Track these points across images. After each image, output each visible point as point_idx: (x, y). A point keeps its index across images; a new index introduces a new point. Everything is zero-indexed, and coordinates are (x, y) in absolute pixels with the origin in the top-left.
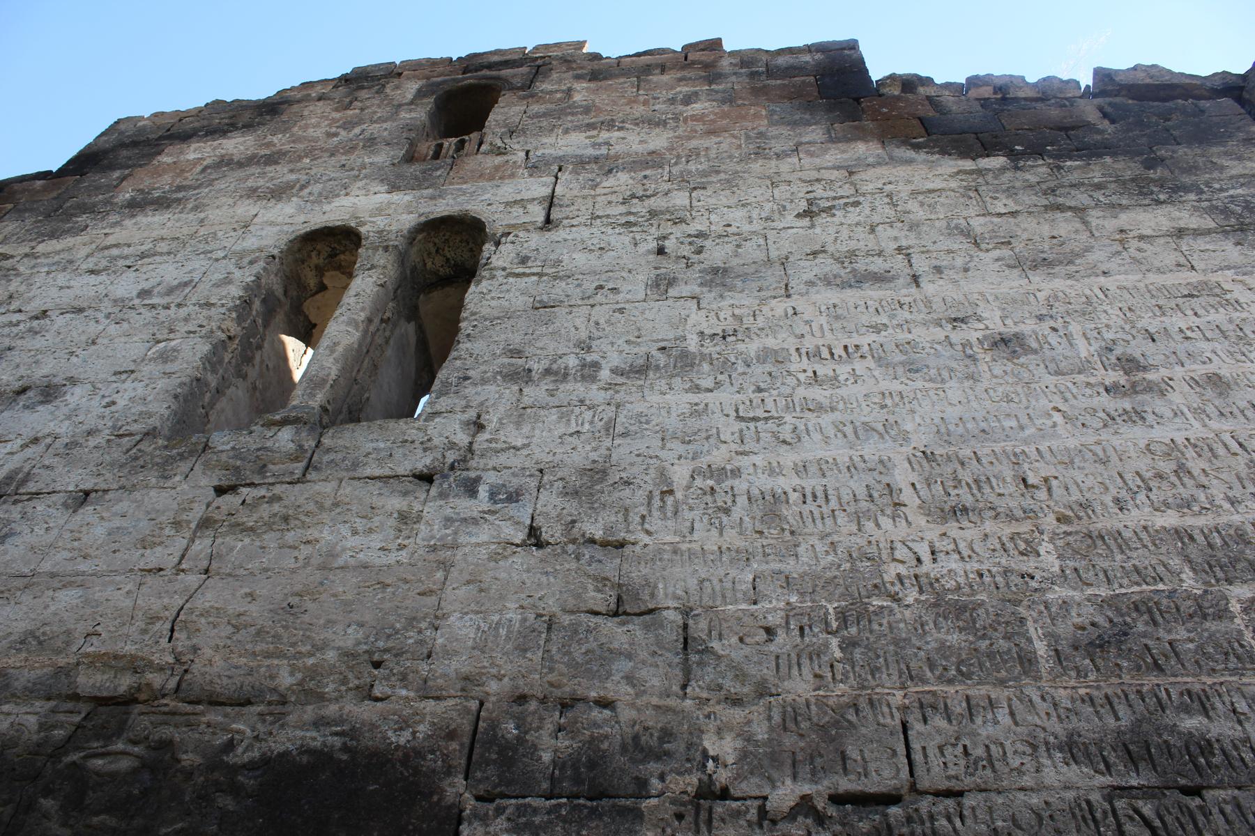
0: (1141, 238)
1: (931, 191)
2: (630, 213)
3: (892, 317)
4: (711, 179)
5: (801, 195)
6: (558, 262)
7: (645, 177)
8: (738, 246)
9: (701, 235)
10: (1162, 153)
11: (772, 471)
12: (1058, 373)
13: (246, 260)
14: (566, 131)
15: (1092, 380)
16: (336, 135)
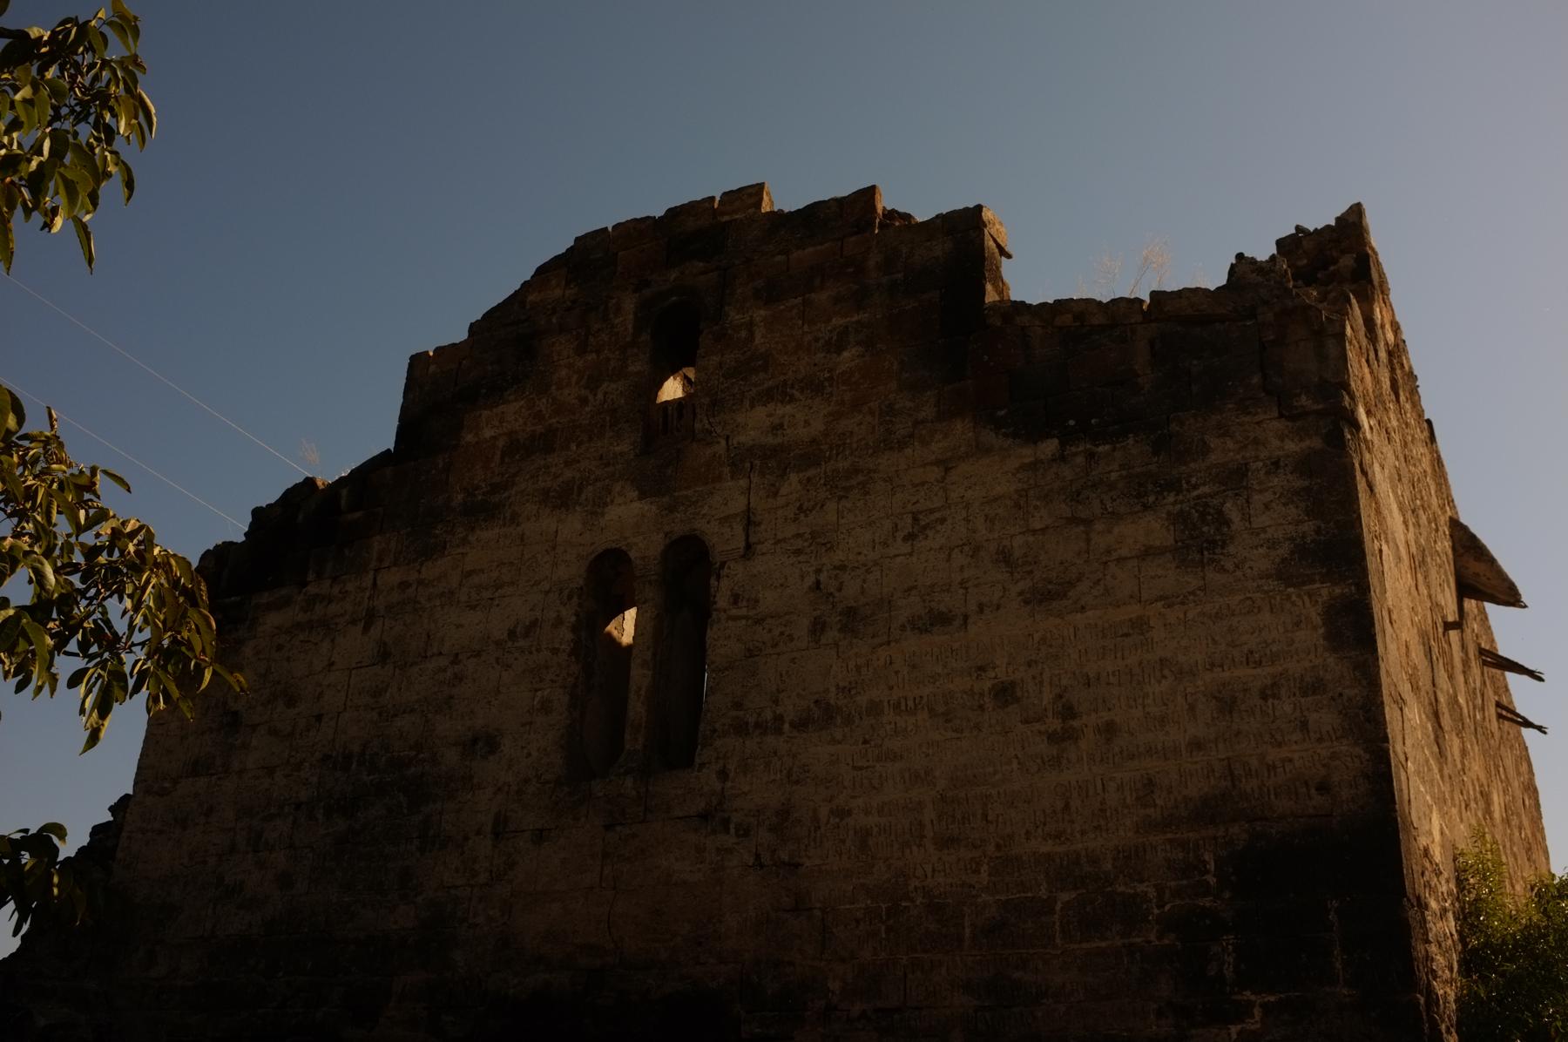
0: (1118, 560)
1: (996, 500)
2: (798, 535)
3: (945, 667)
4: (854, 482)
5: (909, 507)
6: (757, 601)
7: (809, 479)
8: (864, 581)
9: (842, 568)
10: (1174, 427)
11: (867, 813)
12: (1026, 722)
13: (566, 592)
14: (752, 407)
15: (1043, 728)
16: (584, 401)
